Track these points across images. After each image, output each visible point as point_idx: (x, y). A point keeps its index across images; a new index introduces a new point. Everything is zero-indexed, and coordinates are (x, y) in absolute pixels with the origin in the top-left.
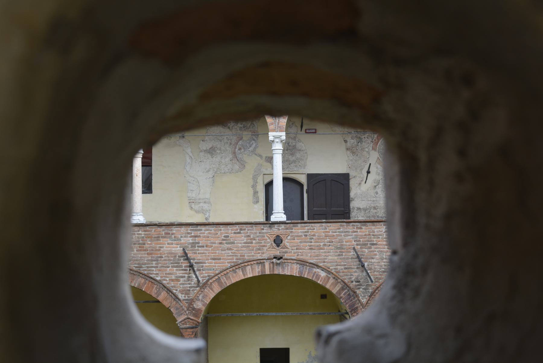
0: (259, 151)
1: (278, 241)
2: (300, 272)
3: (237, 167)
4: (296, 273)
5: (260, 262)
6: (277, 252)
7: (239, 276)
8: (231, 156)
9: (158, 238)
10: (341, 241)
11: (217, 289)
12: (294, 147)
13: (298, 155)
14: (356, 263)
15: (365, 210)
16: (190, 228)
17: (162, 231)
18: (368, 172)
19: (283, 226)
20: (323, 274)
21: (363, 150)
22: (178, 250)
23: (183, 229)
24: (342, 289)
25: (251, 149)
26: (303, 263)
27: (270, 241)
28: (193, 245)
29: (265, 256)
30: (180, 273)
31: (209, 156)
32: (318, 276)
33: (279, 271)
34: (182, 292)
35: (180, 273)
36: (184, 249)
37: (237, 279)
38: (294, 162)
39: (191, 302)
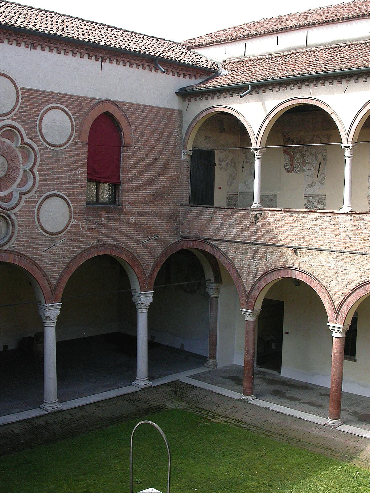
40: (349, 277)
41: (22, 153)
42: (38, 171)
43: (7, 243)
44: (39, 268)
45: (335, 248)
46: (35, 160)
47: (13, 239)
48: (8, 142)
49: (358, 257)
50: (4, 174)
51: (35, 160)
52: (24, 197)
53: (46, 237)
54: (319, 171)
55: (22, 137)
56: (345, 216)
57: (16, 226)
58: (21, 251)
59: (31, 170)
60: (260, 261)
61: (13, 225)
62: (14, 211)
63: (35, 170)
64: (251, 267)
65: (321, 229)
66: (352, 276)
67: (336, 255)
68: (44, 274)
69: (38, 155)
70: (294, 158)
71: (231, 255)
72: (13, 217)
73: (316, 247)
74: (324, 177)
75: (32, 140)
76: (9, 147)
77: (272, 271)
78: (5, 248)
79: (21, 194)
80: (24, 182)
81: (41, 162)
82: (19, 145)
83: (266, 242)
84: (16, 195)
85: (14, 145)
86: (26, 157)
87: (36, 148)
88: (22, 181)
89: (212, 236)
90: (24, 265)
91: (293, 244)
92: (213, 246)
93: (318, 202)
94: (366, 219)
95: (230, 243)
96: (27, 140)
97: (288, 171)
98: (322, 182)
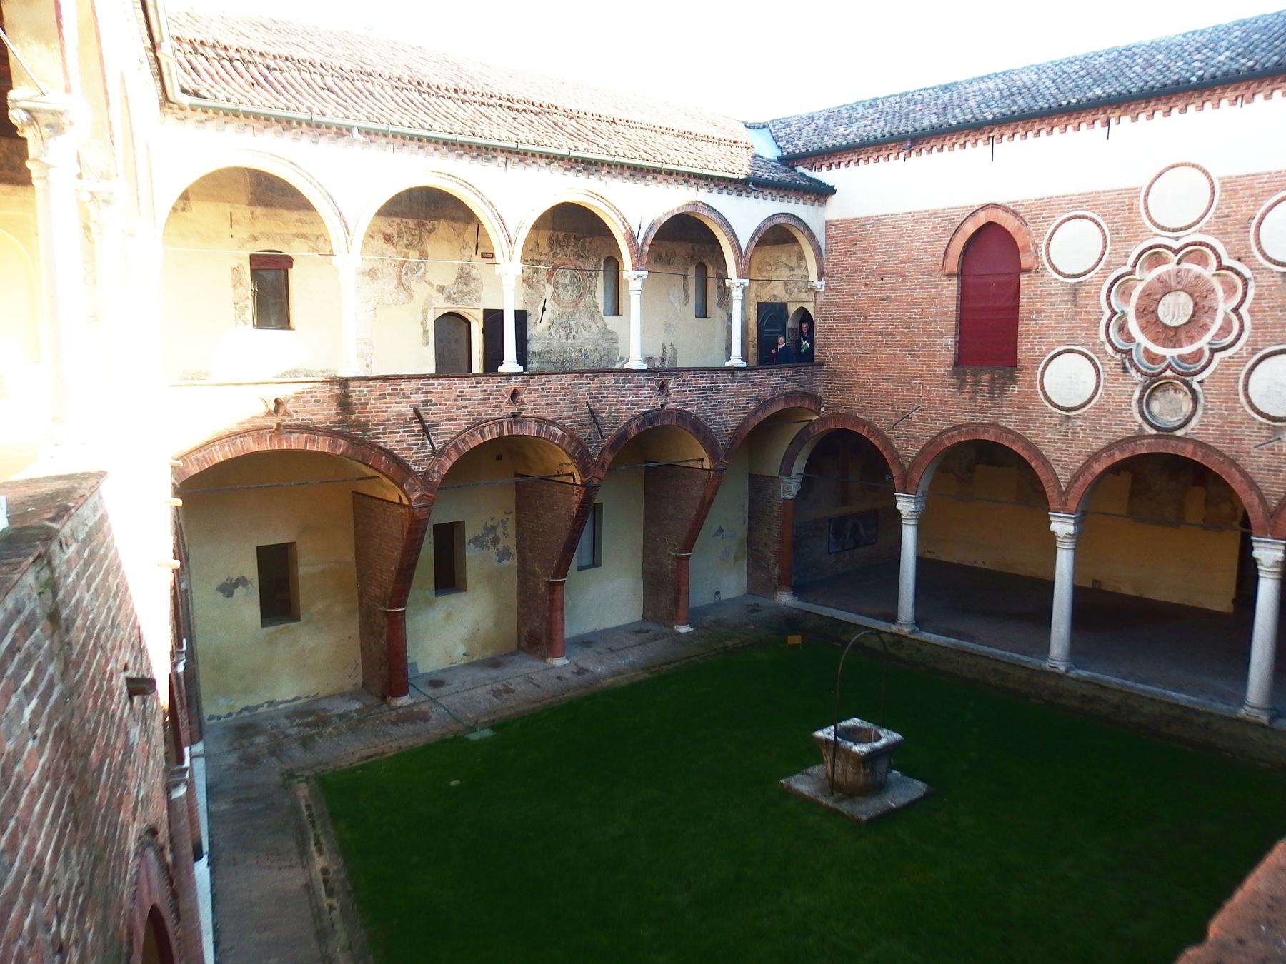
0: (429, 277)
1: (514, 395)
2: (538, 431)
3: (403, 297)
4: (533, 433)
5: (499, 422)
6: (514, 409)
7: (479, 440)
8: (395, 282)
9: (382, 397)
10: (575, 395)
11: (455, 457)
12: (468, 274)
13: (472, 285)
14: (588, 418)
15: (539, 354)
16: (420, 382)
17: (388, 387)
18: (544, 310)
19: (520, 378)
20: (559, 433)
21: (538, 282)
22: (408, 411)
23: (413, 384)
24: (577, 448)
25: (420, 274)
26: (540, 420)
27: (508, 396)
28: (426, 402)
29: (503, 414)
30: (411, 440)
31: (369, 280)
32: (555, 435)
33: (517, 431)
34: (415, 463)
35: (411, 440)
36: (415, 409)
37: (476, 444)
38: (469, 293)
39: (426, 474)
41: (1223, 283)
42: (1251, 311)
43: (1180, 427)
44: (1244, 474)
46: (1245, 295)
47: (1194, 422)
48: (1196, 269)
50: (1186, 320)
51: (1245, 295)
52: (1218, 356)
53: (1262, 424)
55: (1218, 257)
57: (1202, 401)
58: (1209, 440)
59: (1235, 310)
61: (1195, 399)
62: (1199, 378)
63: (1243, 311)
68: (1252, 484)
69: (1251, 284)
72: (1196, 386)
75: (1239, 260)
76: (1198, 277)
78: (1179, 433)
79: (1213, 351)
80: (1226, 329)
81: (1258, 297)
82: (1214, 271)
84: (1207, 353)
85: (1208, 272)
86: (1230, 289)
87: (1247, 273)
88: (1221, 328)
90: (1212, 463)
96: (1226, 261)
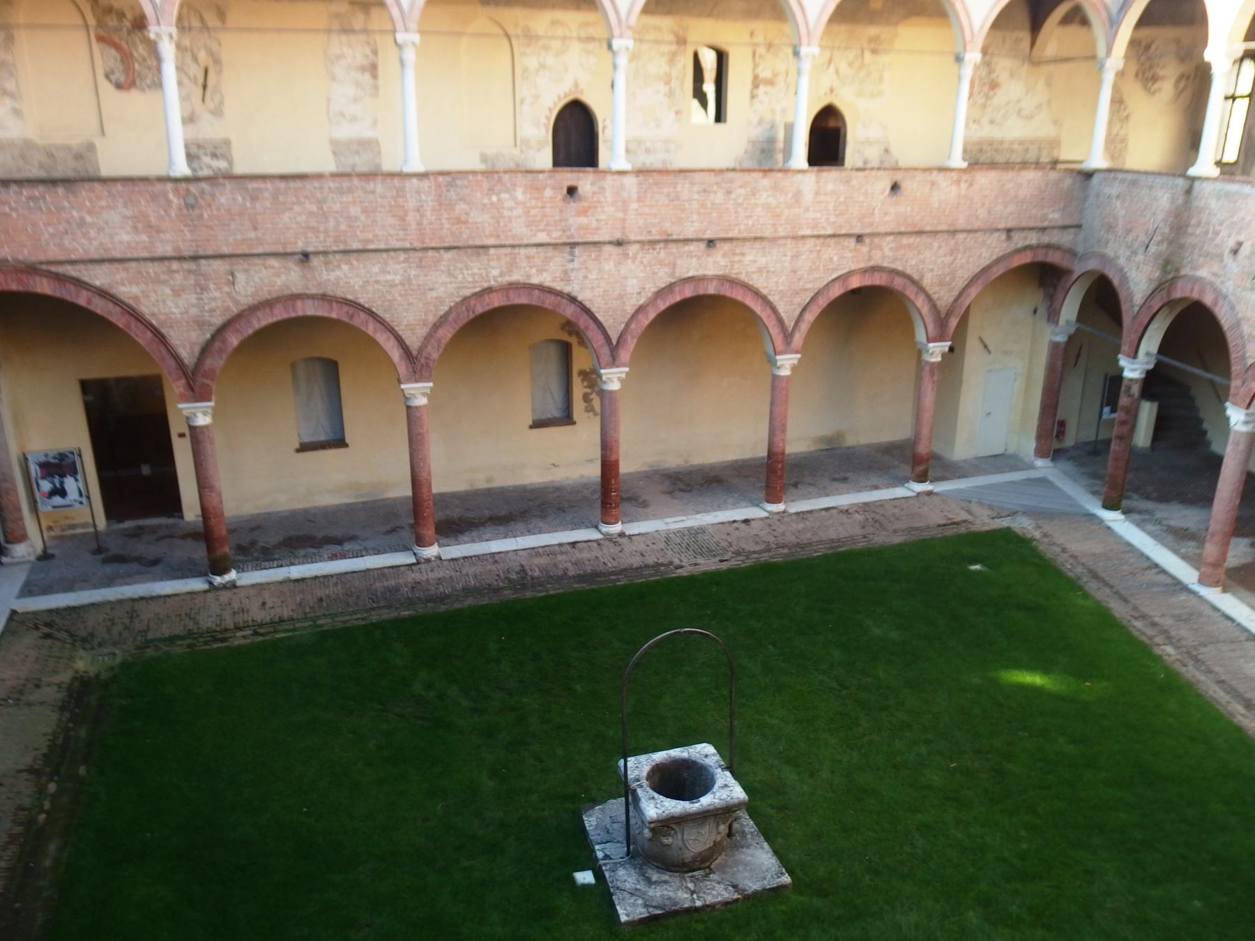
40: (434, 294)
45: (398, 245)
49: (448, 255)
54: (205, 87)
56: (415, 181)
60: (217, 294)
64: (194, 311)
65: (365, 211)
66: (440, 291)
67: (402, 256)
70: (132, 55)
71: (127, 290)
73: (356, 245)
74: (221, 102)
77: (254, 309)
83: (225, 250)
89: (54, 253)
91: (300, 246)
92: (60, 278)
93: (214, 156)
94: (459, 182)
95: (117, 265)
97: (119, 86)
98: (218, 112)
